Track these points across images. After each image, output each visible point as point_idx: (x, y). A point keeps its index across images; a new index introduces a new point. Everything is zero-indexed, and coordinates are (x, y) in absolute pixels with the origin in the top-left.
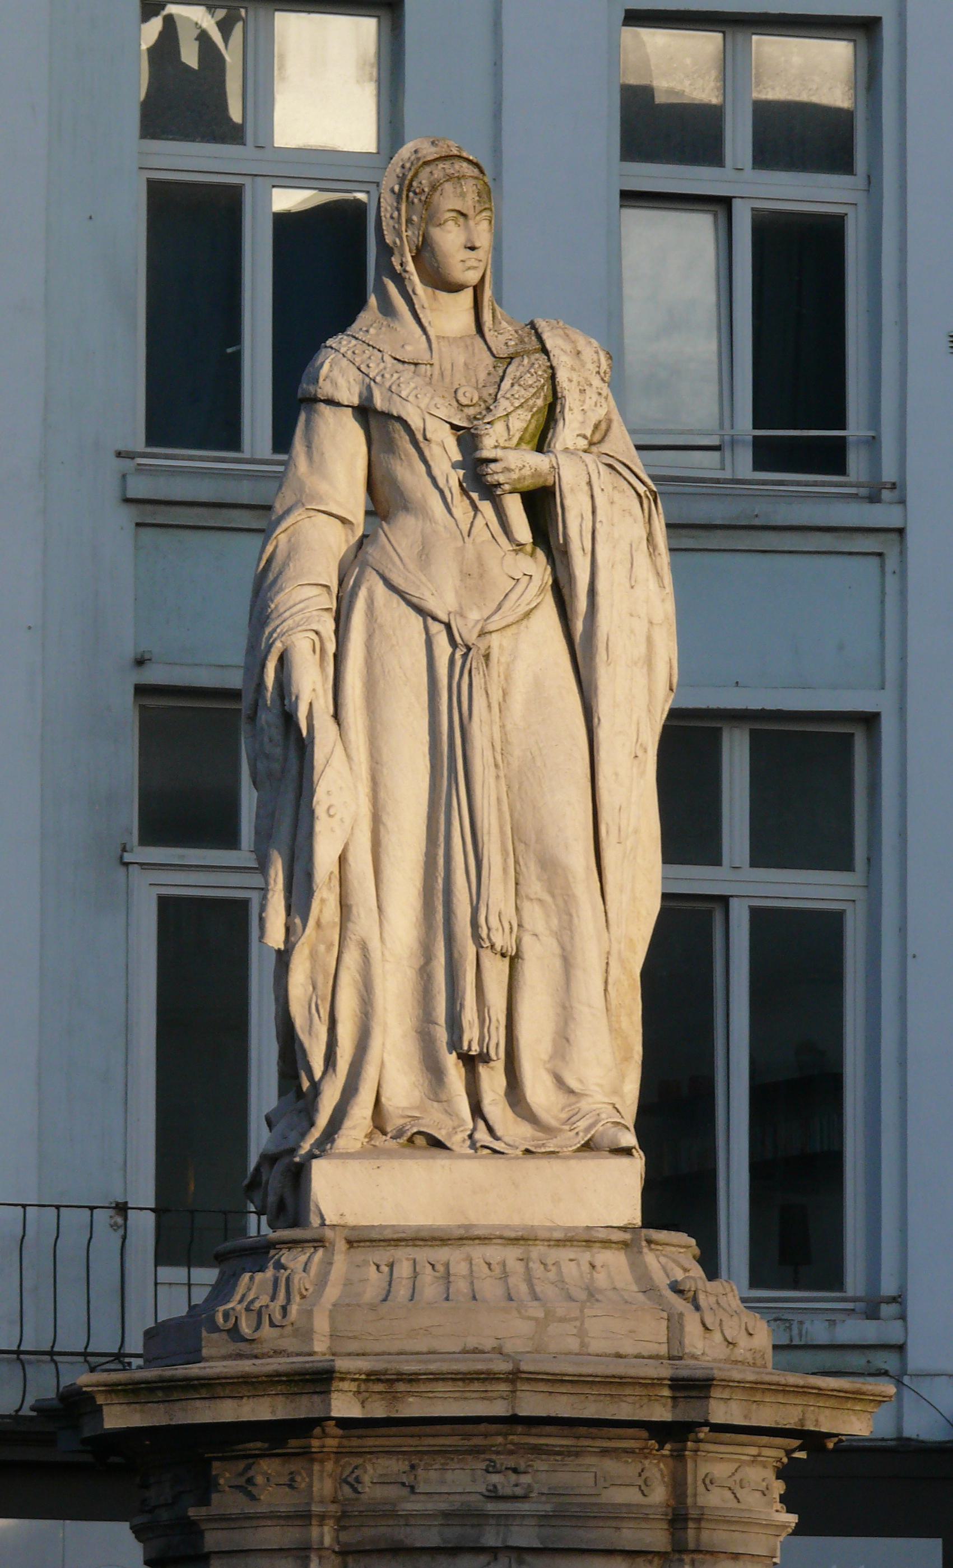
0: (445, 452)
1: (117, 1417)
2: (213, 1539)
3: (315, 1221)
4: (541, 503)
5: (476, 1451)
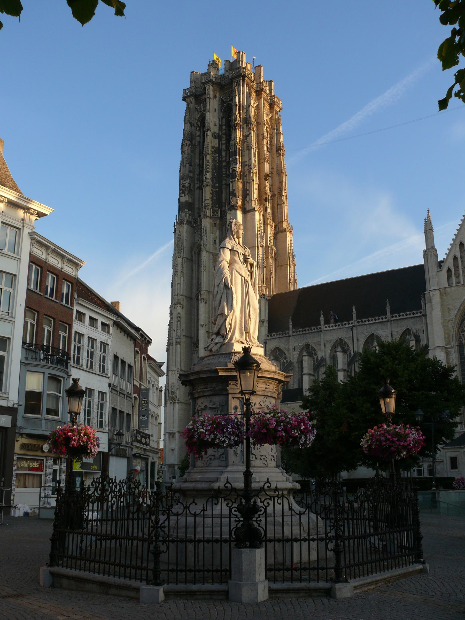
0: (241, 257)
1: (221, 373)
2: (230, 392)
3: (233, 350)
4: (251, 265)
5: (264, 382)
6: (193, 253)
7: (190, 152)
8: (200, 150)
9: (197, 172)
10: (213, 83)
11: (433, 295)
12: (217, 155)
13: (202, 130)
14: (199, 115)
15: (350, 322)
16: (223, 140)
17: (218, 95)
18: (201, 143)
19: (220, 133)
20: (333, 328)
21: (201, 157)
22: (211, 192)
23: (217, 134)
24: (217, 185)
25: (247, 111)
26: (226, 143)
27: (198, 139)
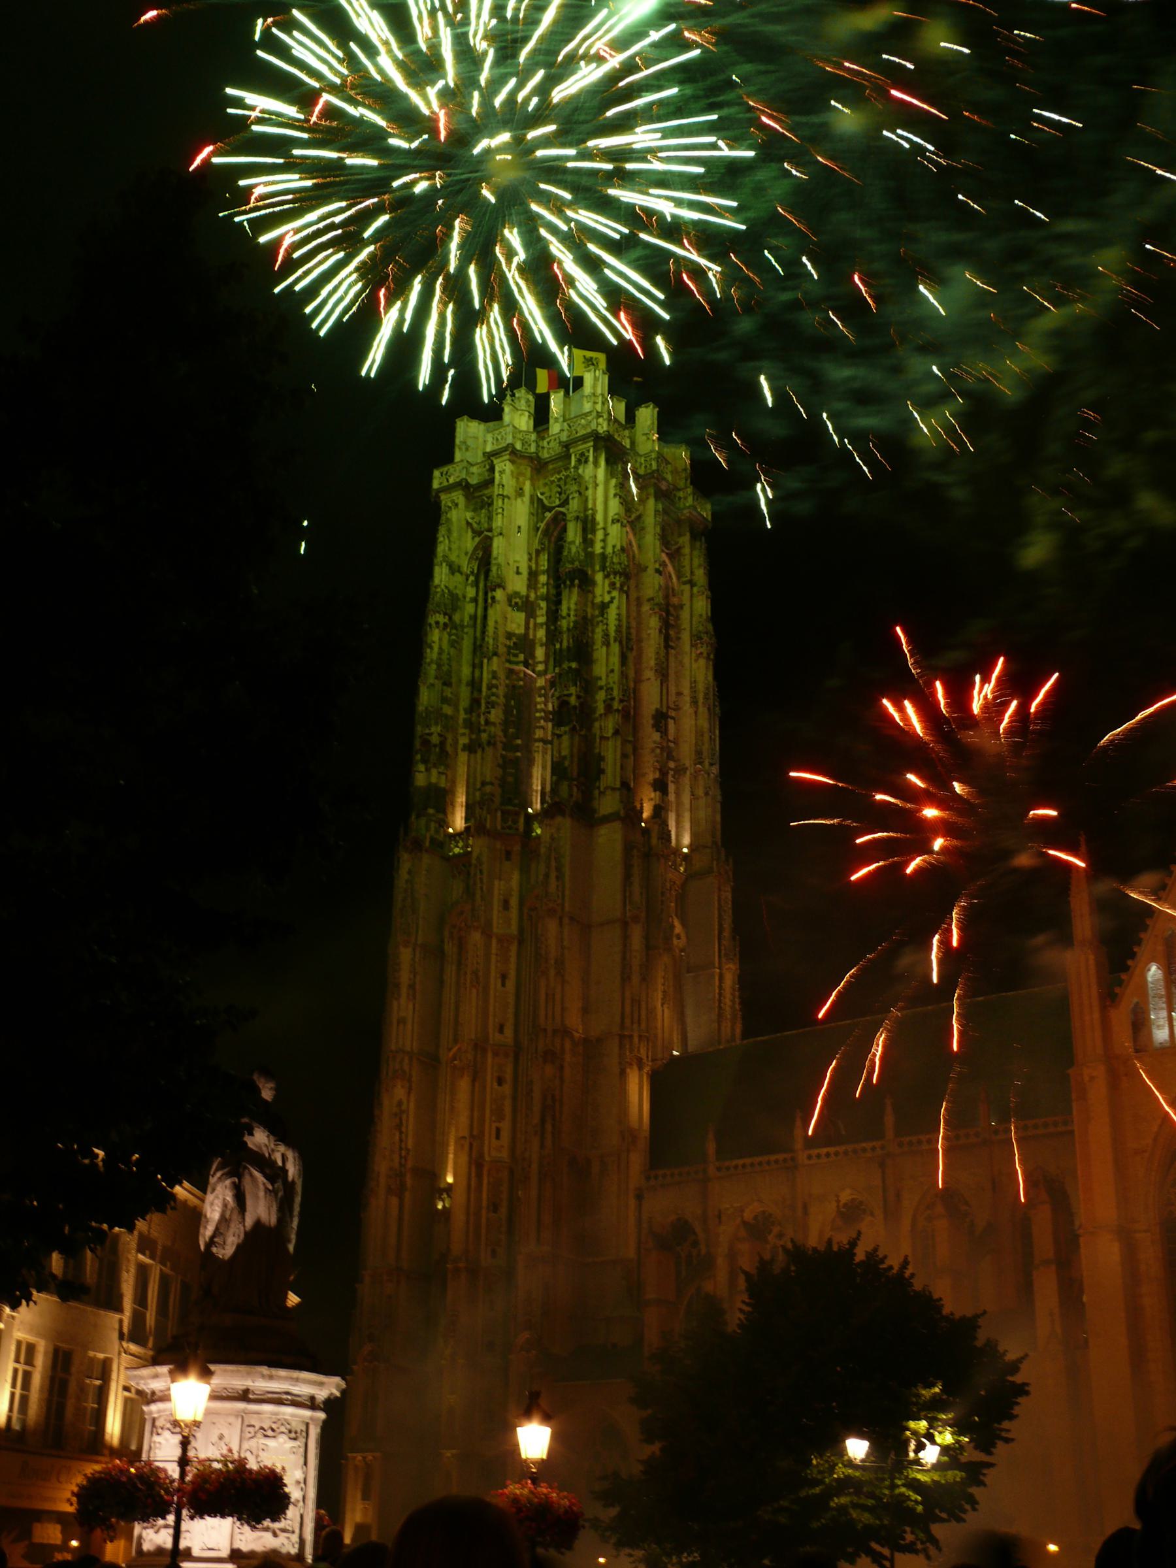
6: (446, 934)
7: (445, 646)
8: (475, 638)
9: (464, 703)
10: (515, 454)
11: (1092, 1078)
12: (521, 657)
13: (481, 585)
14: (477, 539)
15: (877, 1144)
16: (539, 613)
17: (527, 487)
18: (479, 621)
19: (532, 596)
20: (812, 1162)
21: (477, 661)
22: (501, 761)
23: (521, 598)
24: (519, 742)
25: (606, 535)
26: (546, 624)
27: (470, 608)
